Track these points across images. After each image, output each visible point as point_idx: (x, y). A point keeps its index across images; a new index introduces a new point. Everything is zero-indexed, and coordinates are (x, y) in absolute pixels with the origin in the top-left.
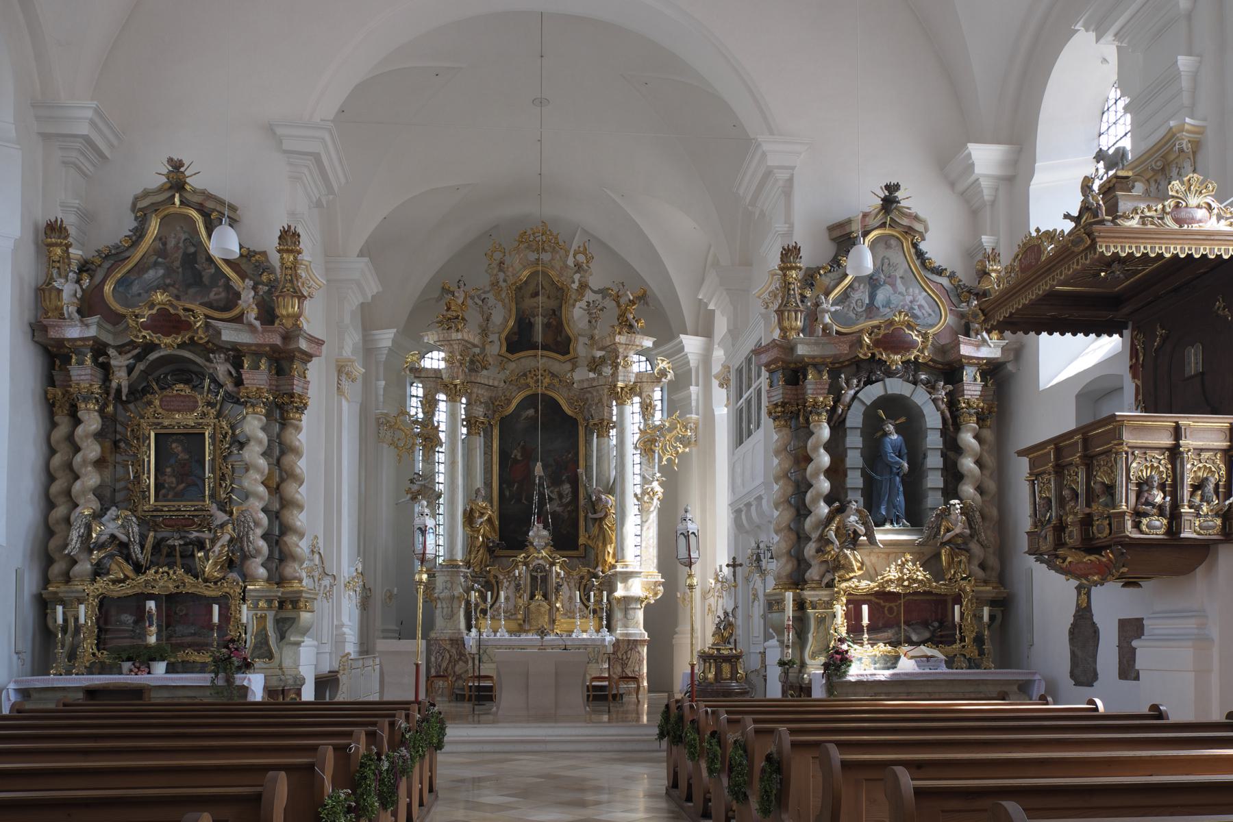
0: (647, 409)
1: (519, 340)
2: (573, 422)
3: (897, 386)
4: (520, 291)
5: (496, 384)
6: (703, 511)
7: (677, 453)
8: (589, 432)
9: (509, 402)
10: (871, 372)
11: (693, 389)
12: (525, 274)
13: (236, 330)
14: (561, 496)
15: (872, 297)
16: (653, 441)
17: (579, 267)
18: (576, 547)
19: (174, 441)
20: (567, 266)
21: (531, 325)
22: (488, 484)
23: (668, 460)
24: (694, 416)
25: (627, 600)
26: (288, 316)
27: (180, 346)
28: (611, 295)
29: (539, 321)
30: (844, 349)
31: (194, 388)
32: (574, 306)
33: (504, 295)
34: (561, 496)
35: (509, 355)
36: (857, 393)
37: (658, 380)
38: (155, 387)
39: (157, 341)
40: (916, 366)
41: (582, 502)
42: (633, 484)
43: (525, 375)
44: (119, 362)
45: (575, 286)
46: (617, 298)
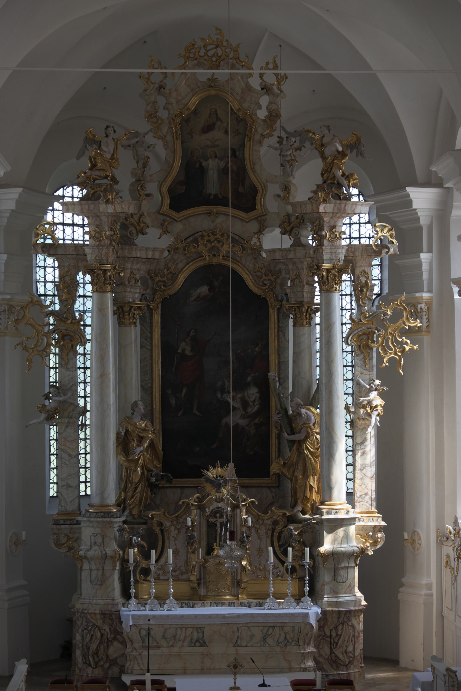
0: (361, 289)
1: (188, 192)
2: (262, 304)
4: (186, 124)
5: (157, 255)
6: (439, 423)
7: (403, 350)
8: (282, 317)
9: (174, 276)
11: (424, 257)
12: (194, 102)
14: (245, 404)
16: (369, 335)
17: (266, 89)
18: (266, 474)
20: (249, 88)
21: (202, 171)
22: (147, 389)
23: (389, 361)
24: (425, 295)
25: (334, 556)
28: (312, 141)
29: (212, 166)
32: (260, 143)
33: (165, 129)
34: (245, 404)
35: (174, 214)
37: (377, 254)
41: (275, 417)
42: (342, 396)
45: (262, 114)
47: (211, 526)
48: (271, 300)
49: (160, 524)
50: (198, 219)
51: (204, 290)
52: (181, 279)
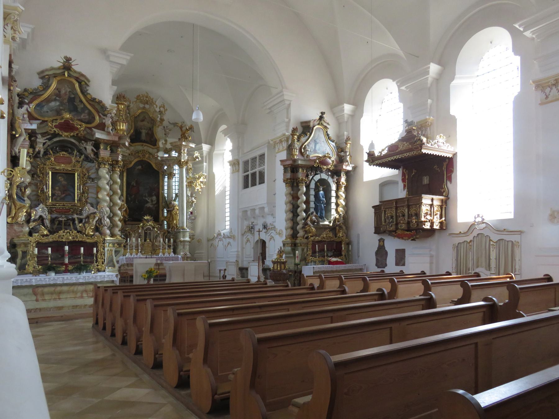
3: (324, 176)
9: (131, 162)
10: (316, 171)
13: (102, 133)
14: (152, 201)
15: (315, 147)
17: (160, 112)
19: (60, 176)
25: (184, 241)
26: (120, 130)
27: (72, 137)
29: (144, 132)
30: (312, 163)
31: (69, 153)
34: (152, 201)
36: (313, 177)
38: (51, 152)
39: (61, 134)
40: (328, 170)
43: (138, 152)
44: (40, 140)
46: (181, 128)
47: (146, 233)
48: (160, 172)
49: (129, 232)
50: (138, 147)
51: (140, 167)
52: (133, 163)
